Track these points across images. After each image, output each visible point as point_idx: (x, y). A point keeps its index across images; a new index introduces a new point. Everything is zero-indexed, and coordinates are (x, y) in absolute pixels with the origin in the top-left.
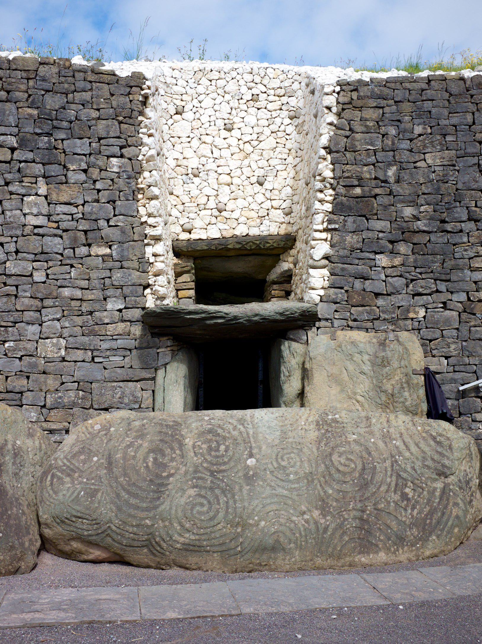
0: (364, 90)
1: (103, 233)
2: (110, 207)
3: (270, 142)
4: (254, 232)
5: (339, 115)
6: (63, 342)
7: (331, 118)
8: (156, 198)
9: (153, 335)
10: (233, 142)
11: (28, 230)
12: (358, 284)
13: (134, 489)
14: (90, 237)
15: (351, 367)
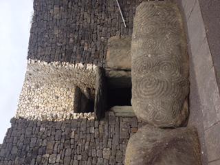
0: (32, 51)
1: (67, 134)
2: (58, 131)
3: (45, 95)
4: (73, 100)
5: (38, 59)
6: (105, 149)
7: (39, 61)
8: (56, 115)
9: (104, 117)
10: (43, 106)
11: (62, 161)
12: (92, 56)
13: (160, 90)
14: (68, 138)
15: (118, 55)
